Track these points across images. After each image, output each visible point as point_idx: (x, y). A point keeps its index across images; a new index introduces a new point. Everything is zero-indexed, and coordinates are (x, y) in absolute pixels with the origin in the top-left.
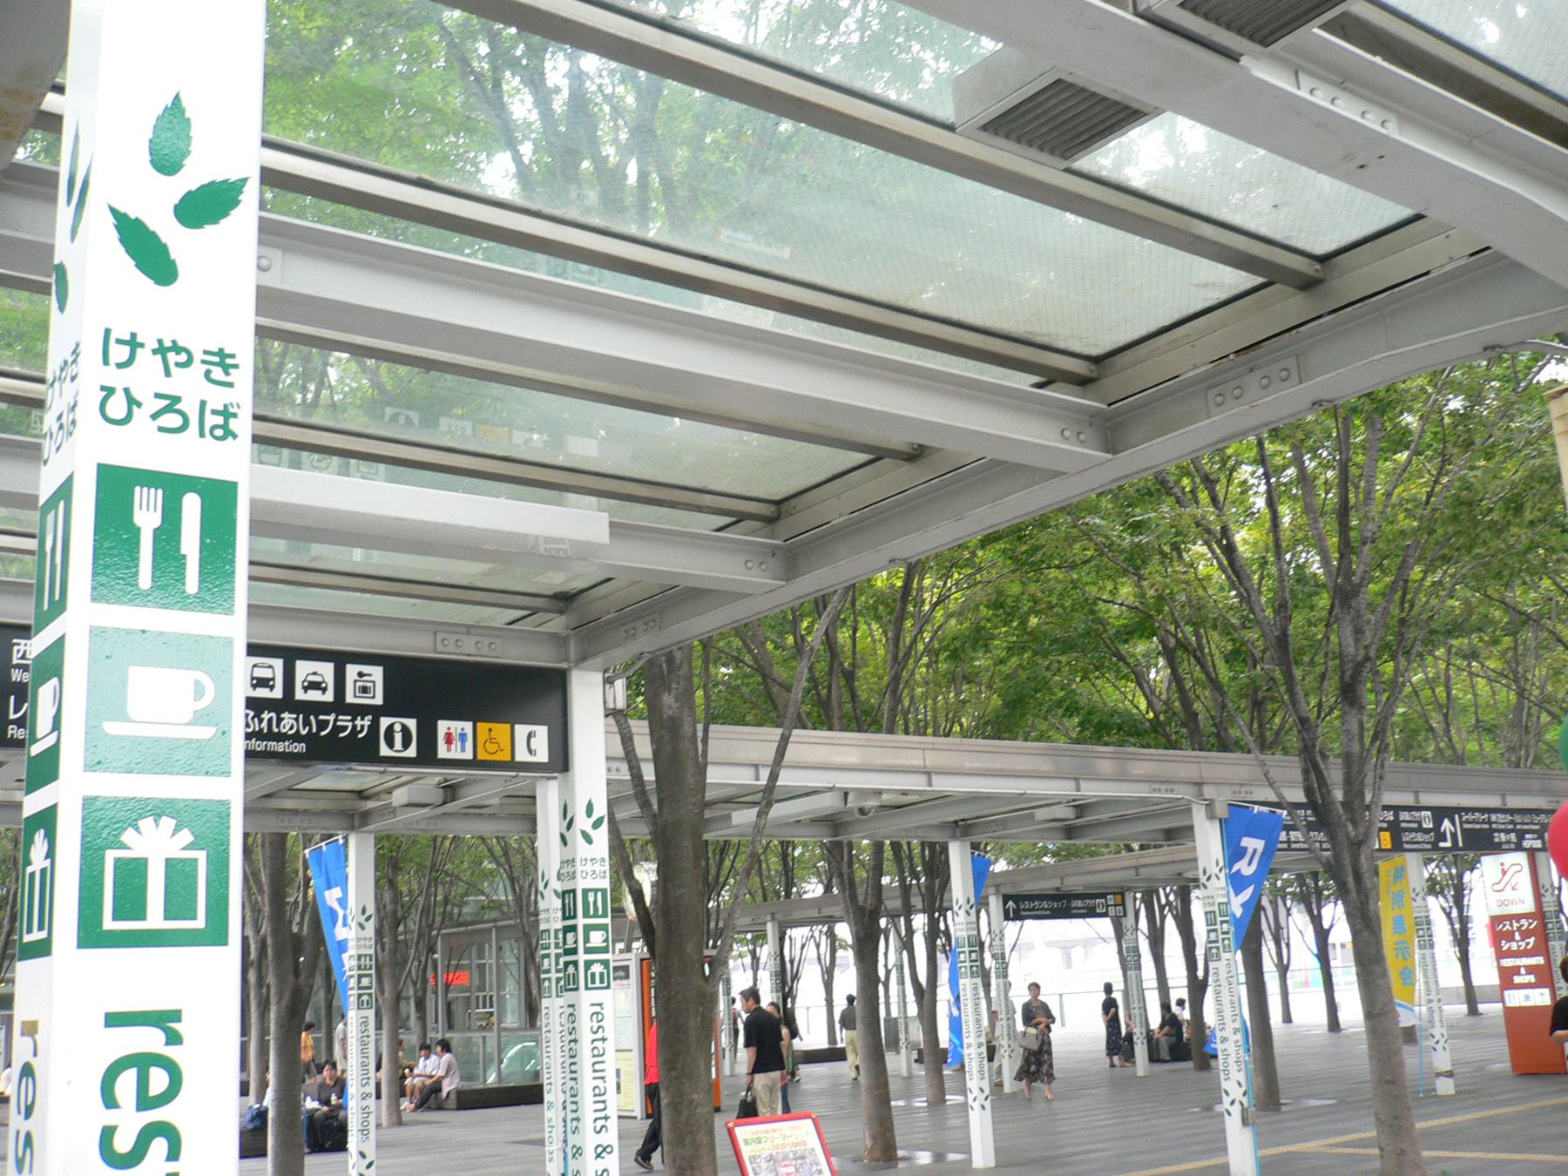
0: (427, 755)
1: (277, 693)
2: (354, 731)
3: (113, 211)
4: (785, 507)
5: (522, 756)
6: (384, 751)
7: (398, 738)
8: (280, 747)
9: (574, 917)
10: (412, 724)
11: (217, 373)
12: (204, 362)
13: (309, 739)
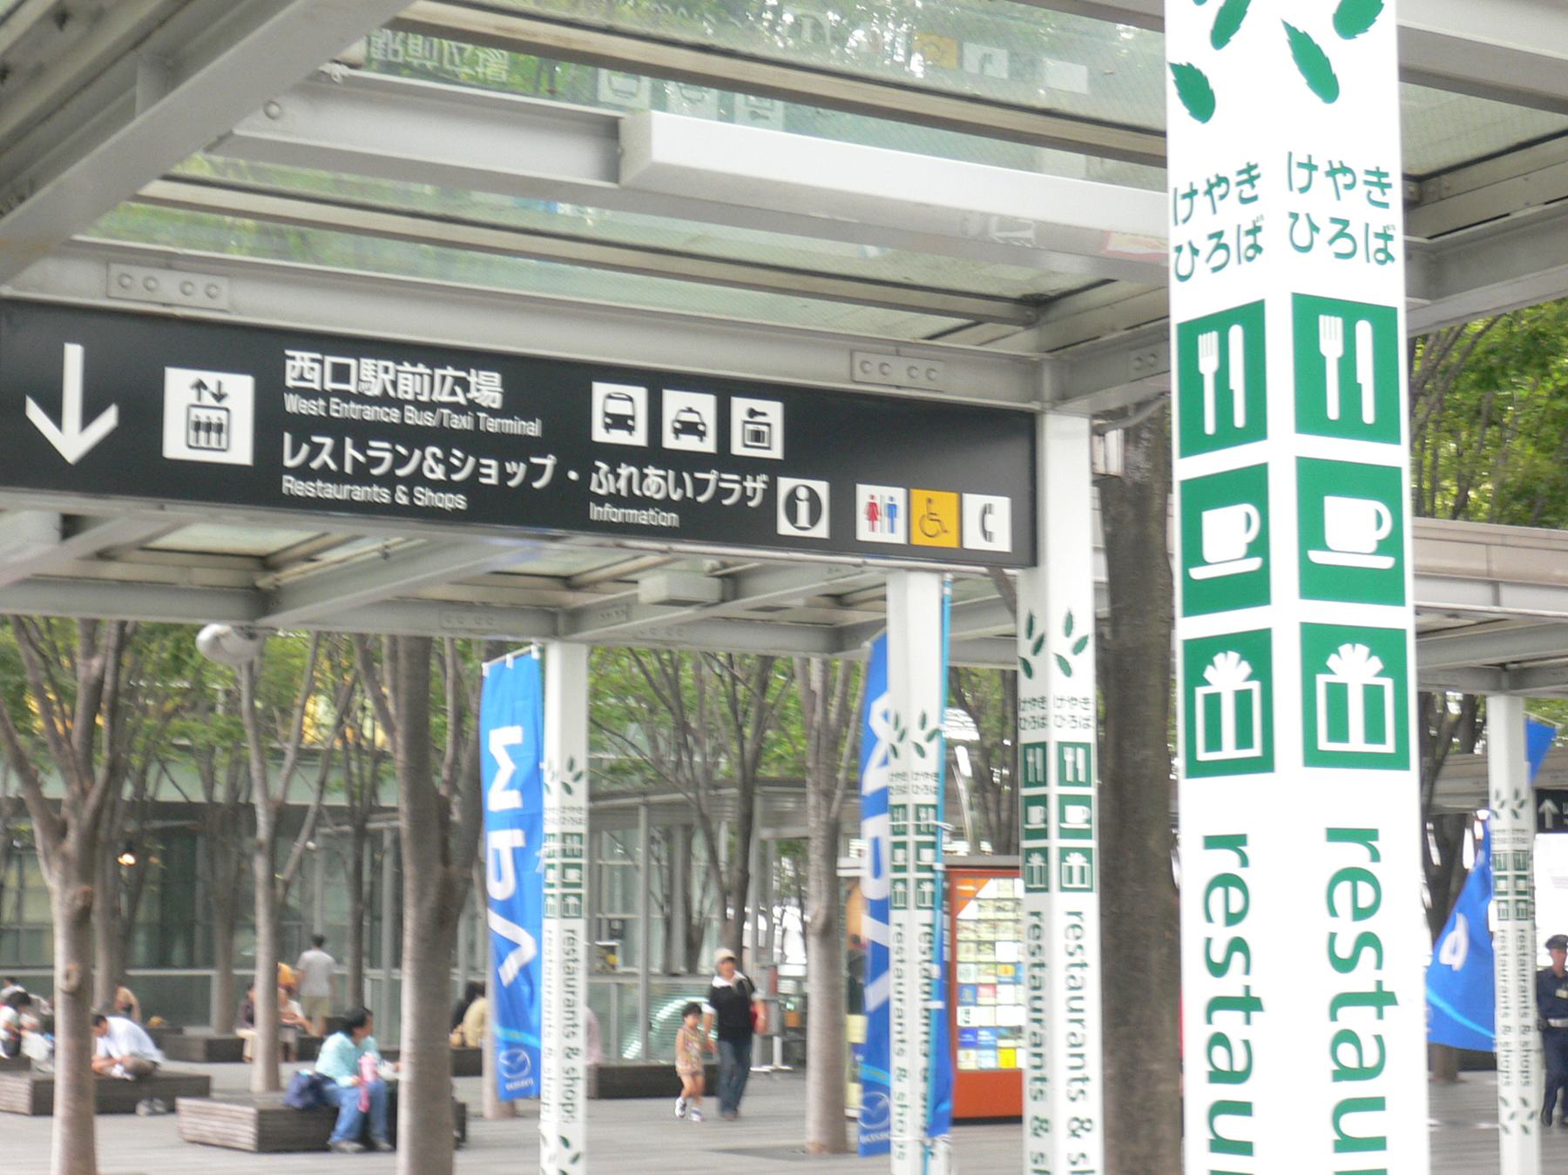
0: (843, 539)
1: (639, 438)
2: (745, 498)
3: (1286, 25)
4: (1431, 186)
5: (974, 541)
6: (784, 527)
7: (803, 509)
8: (644, 517)
9: (1044, 783)
10: (822, 488)
11: (1376, 194)
12: (1367, 183)
13: (683, 507)
